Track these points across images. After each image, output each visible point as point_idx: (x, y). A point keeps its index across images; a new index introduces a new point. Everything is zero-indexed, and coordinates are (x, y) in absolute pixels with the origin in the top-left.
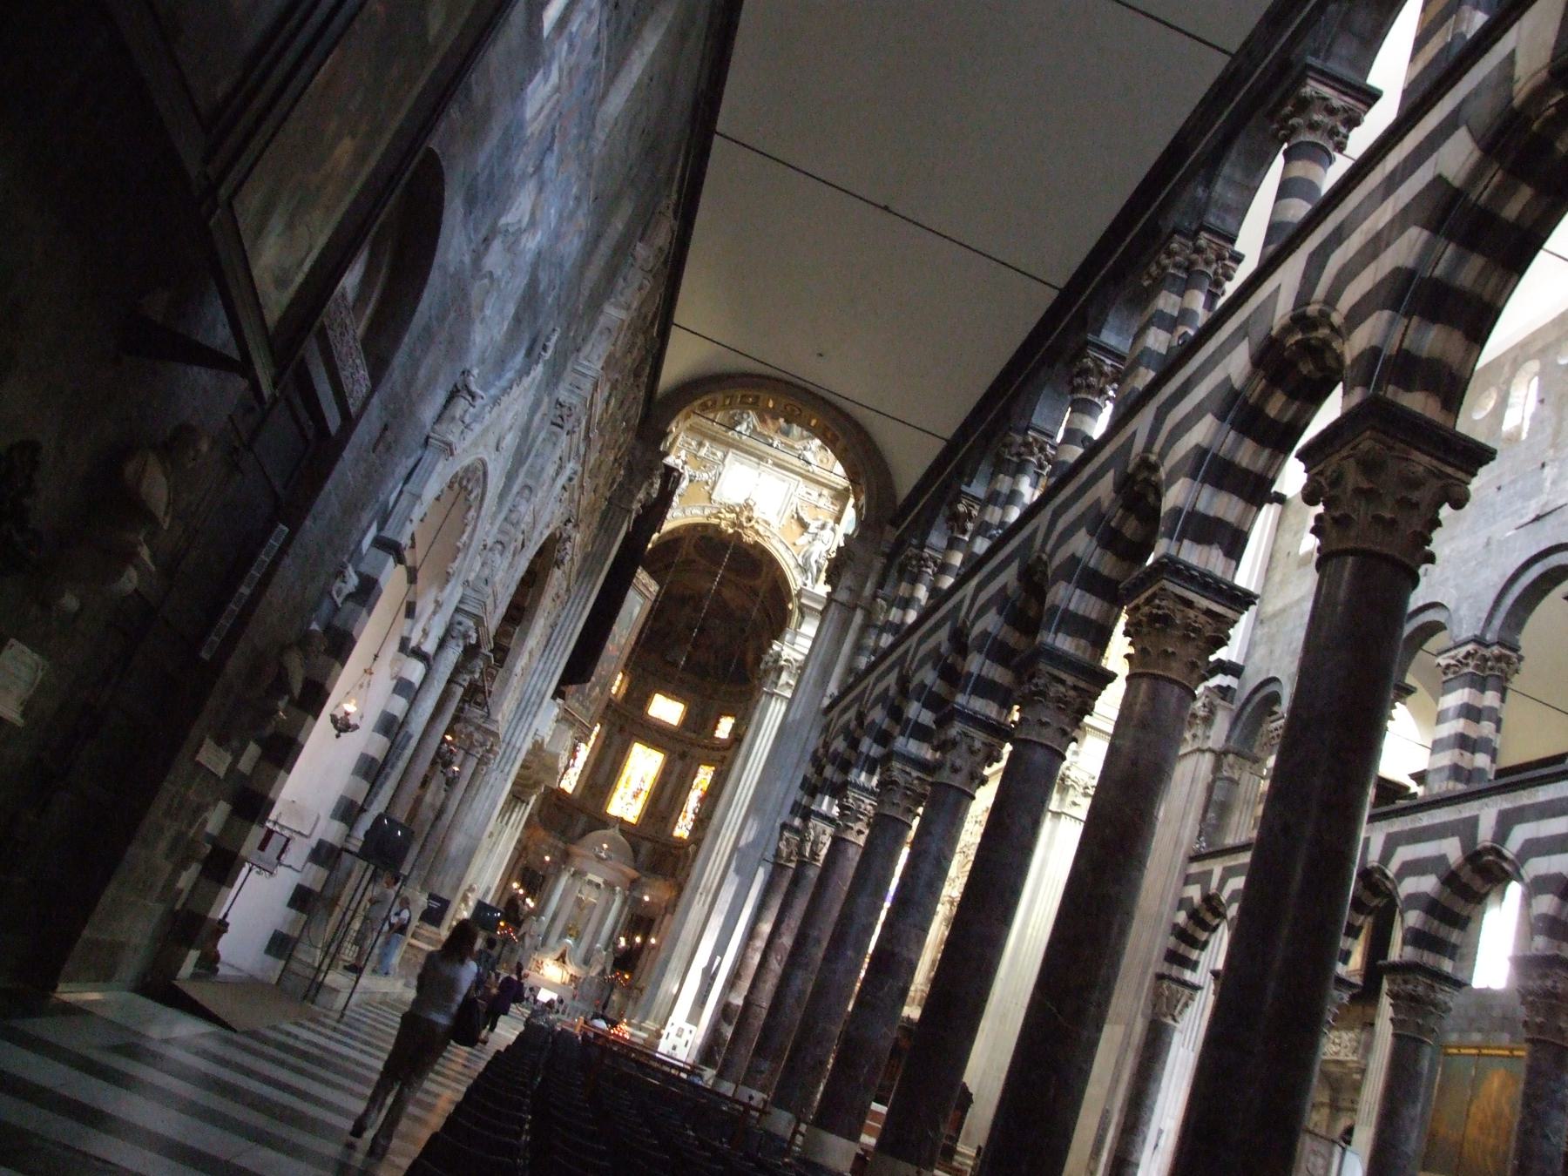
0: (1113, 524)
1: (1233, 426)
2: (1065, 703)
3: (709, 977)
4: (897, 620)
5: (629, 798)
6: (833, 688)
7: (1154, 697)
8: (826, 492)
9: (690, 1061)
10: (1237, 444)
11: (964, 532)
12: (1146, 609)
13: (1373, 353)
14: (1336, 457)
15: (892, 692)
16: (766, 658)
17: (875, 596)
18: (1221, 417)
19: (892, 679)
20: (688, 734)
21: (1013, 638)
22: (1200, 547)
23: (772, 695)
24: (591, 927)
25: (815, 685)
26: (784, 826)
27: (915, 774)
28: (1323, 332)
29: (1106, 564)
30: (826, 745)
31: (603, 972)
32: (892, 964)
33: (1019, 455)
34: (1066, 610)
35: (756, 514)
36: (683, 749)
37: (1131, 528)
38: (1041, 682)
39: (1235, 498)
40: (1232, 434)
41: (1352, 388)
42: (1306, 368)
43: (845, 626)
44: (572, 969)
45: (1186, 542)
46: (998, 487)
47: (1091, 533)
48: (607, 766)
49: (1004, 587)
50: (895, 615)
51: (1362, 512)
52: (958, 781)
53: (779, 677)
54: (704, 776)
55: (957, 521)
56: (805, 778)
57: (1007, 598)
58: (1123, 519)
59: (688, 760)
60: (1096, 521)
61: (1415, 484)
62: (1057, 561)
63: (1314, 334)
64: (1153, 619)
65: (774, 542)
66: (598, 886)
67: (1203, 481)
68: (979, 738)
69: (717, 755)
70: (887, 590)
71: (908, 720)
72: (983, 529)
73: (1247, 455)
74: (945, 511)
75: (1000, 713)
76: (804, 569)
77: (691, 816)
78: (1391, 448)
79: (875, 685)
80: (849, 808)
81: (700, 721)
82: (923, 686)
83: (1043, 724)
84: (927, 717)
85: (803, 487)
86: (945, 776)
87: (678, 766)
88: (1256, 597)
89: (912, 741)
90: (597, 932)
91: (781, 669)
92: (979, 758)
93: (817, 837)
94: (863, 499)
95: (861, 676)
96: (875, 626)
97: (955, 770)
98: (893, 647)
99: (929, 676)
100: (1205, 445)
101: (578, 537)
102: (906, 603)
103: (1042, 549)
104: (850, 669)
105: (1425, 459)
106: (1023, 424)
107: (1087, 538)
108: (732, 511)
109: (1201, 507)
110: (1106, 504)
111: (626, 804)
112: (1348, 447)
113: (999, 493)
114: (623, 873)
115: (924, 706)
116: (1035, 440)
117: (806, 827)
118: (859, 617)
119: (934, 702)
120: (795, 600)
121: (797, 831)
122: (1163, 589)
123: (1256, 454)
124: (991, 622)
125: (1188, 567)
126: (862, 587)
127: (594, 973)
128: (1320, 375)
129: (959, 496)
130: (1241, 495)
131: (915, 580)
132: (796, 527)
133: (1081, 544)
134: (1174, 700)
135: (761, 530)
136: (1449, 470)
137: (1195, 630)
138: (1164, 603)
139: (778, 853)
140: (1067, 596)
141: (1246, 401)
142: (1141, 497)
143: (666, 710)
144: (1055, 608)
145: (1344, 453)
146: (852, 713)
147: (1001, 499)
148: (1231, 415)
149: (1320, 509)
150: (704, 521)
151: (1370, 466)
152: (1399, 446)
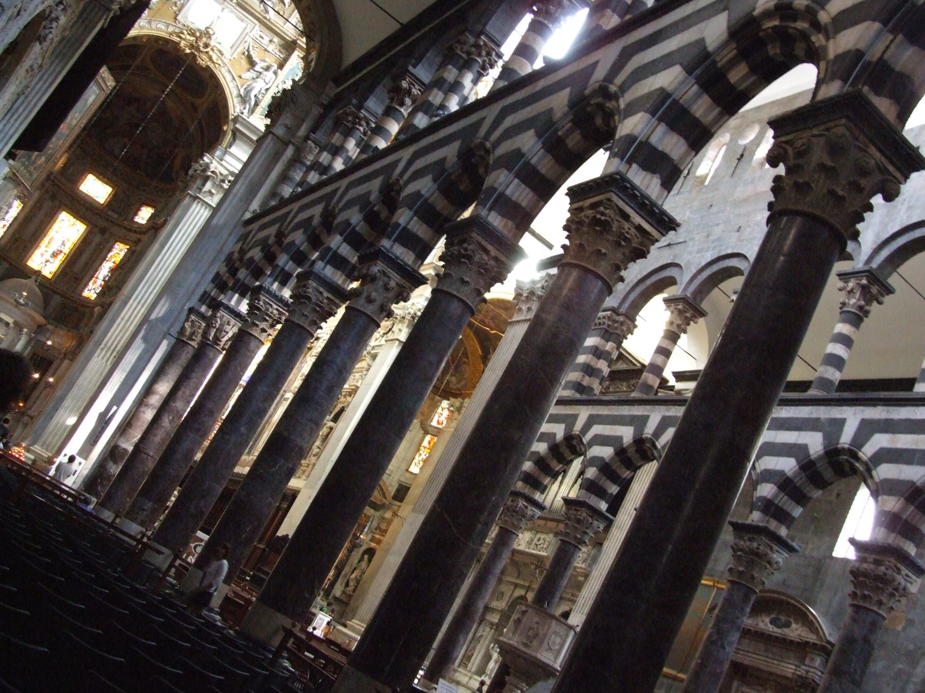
0: (560, 133)
1: (698, 81)
2: (485, 269)
3: (104, 421)
4: (325, 163)
5: (48, 256)
6: (255, 205)
7: (580, 285)
8: (276, 39)
9: (75, 487)
10: (697, 97)
11: (402, 104)
12: (590, 212)
13: (857, 55)
14: (806, 134)
15: (315, 222)
16: (196, 166)
17: (307, 138)
18: (689, 70)
19: (317, 210)
20: (110, 213)
21: (440, 204)
22: (644, 173)
23: (195, 198)
25: (241, 200)
26: (191, 310)
27: (326, 294)
28: (802, 25)
29: (543, 163)
30: (242, 252)
32: (286, 450)
33: (469, 53)
34: (502, 194)
35: (212, 43)
36: (104, 224)
37: (574, 141)
38: (470, 247)
39: (682, 141)
40: (695, 88)
41: (832, 79)
42: (774, 50)
43: (276, 157)
45: (634, 166)
46: (445, 75)
47: (539, 135)
48: (32, 227)
49: (443, 161)
50: (325, 158)
51: (820, 184)
52: (370, 310)
53: (204, 185)
54: (119, 252)
55: (397, 95)
56: (217, 274)
57: (444, 170)
58: (570, 132)
59: (107, 235)
60: (545, 127)
61: (864, 172)
62: (501, 151)
63: (792, 25)
64: (596, 222)
65: (223, 70)
66: (7, 324)
67: (660, 120)
68: (395, 279)
69: (135, 237)
70: (318, 136)
71: (329, 249)
72: (423, 106)
73: (702, 108)
74: (387, 81)
75: (415, 262)
76: (244, 100)
77: (100, 282)
78: (857, 139)
79: (297, 213)
80: (259, 309)
81: (123, 205)
82: (347, 223)
83: (463, 282)
84: (345, 250)
85: (257, 30)
86: (361, 304)
87: (98, 238)
88: (678, 225)
89: (329, 267)
91: (207, 178)
92: (391, 295)
93: (222, 325)
94: (314, 55)
95: (284, 203)
96: (303, 164)
97: (370, 301)
98: (320, 185)
99: (355, 217)
100: (669, 89)
101: (63, 20)
102: (337, 151)
103: (486, 137)
104: (273, 194)
105: (878, 155)
106: (479, 28)
107: (535, 139)
108: (193, 35)
109: (653, 140)
110: (558, 115)
111: (45, 259)
112: (822, 127)
113: (445, 80)
114: (33, 318)
115: (345, 240)
116: (485, 44)
117: (214, 316)
118: (290, 152)
119: (354, 240)
120: (231, 124)
121: (202, 316)
122: (609, 200)
123: (709, 110)
124: (425, 186)
125: (634, 187)
126: (299, 128)
128: (782, 59)
129: (405, 73)
130: (686, 138)
131: (348, 133)
132: (244, 63)
133: (528, 142)
134: (596, 291)
135: (214, 58)
136: (891, 168)
137: (625, 239)
138: (607, 211)
139: (182, 330)
140: (504, 181)
141: (715, 62)
142: (591, 117)
143: (96, 189)
144: (493, 189)
145: (815, 132)
146: (272, 230)
147: (446, 86)
148: (698, 72)
149: (781, 170)
150: (167, 36)
151: (835, 149)
152: (861, 137)
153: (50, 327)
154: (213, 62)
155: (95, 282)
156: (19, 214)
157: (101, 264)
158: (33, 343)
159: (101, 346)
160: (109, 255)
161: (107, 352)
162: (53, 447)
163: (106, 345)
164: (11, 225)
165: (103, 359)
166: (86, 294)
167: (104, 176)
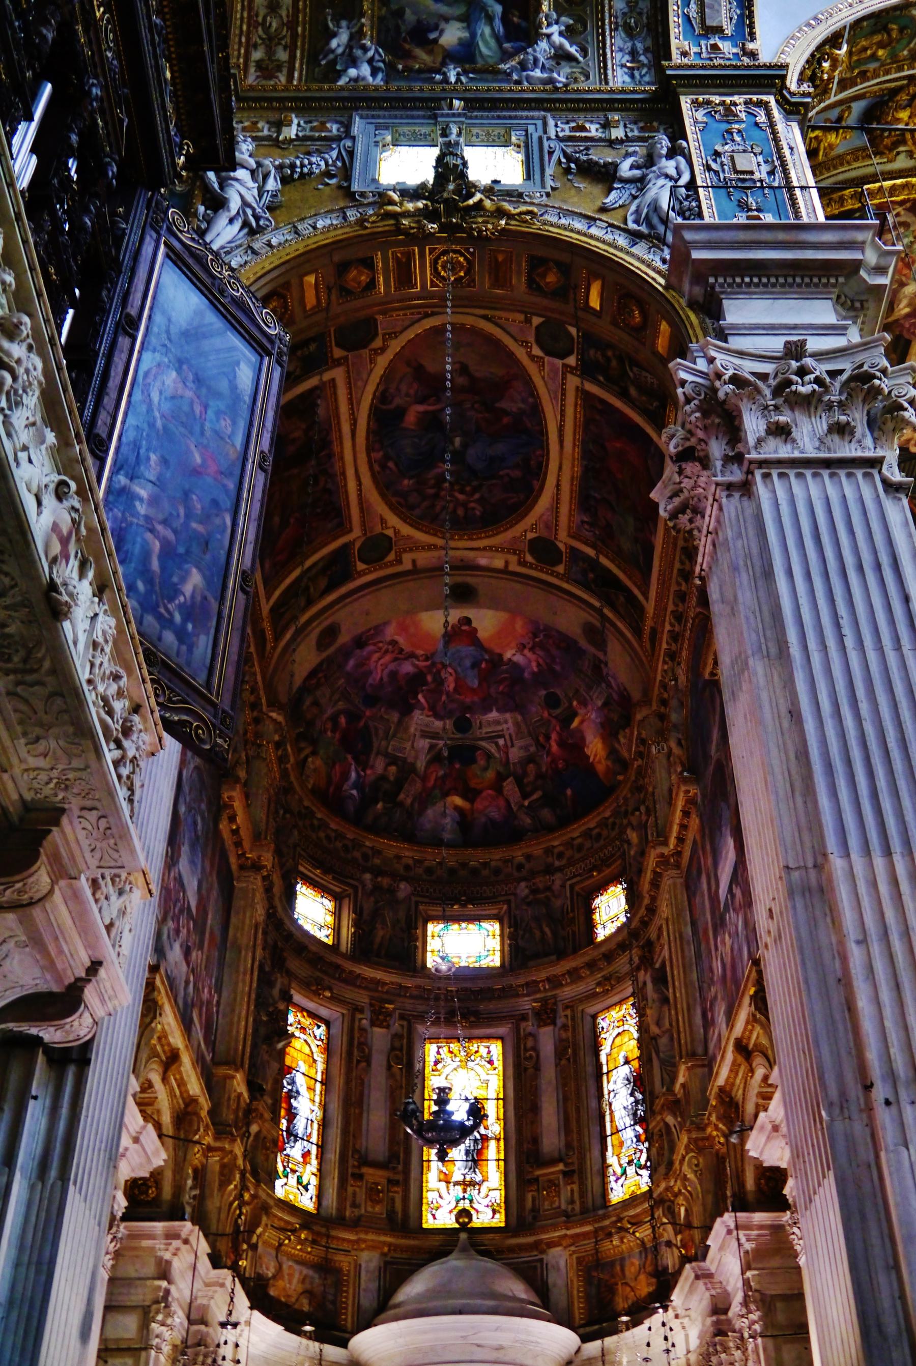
54: (619, 1035)
81: (546, 934)
143: (465, 945)
154: (510, 216)
156: (325, 1107)
157: (602, 1095)
159: (880, 1092)
160: (603, 1059)
164: (321, 1147)
167: (462, 906)
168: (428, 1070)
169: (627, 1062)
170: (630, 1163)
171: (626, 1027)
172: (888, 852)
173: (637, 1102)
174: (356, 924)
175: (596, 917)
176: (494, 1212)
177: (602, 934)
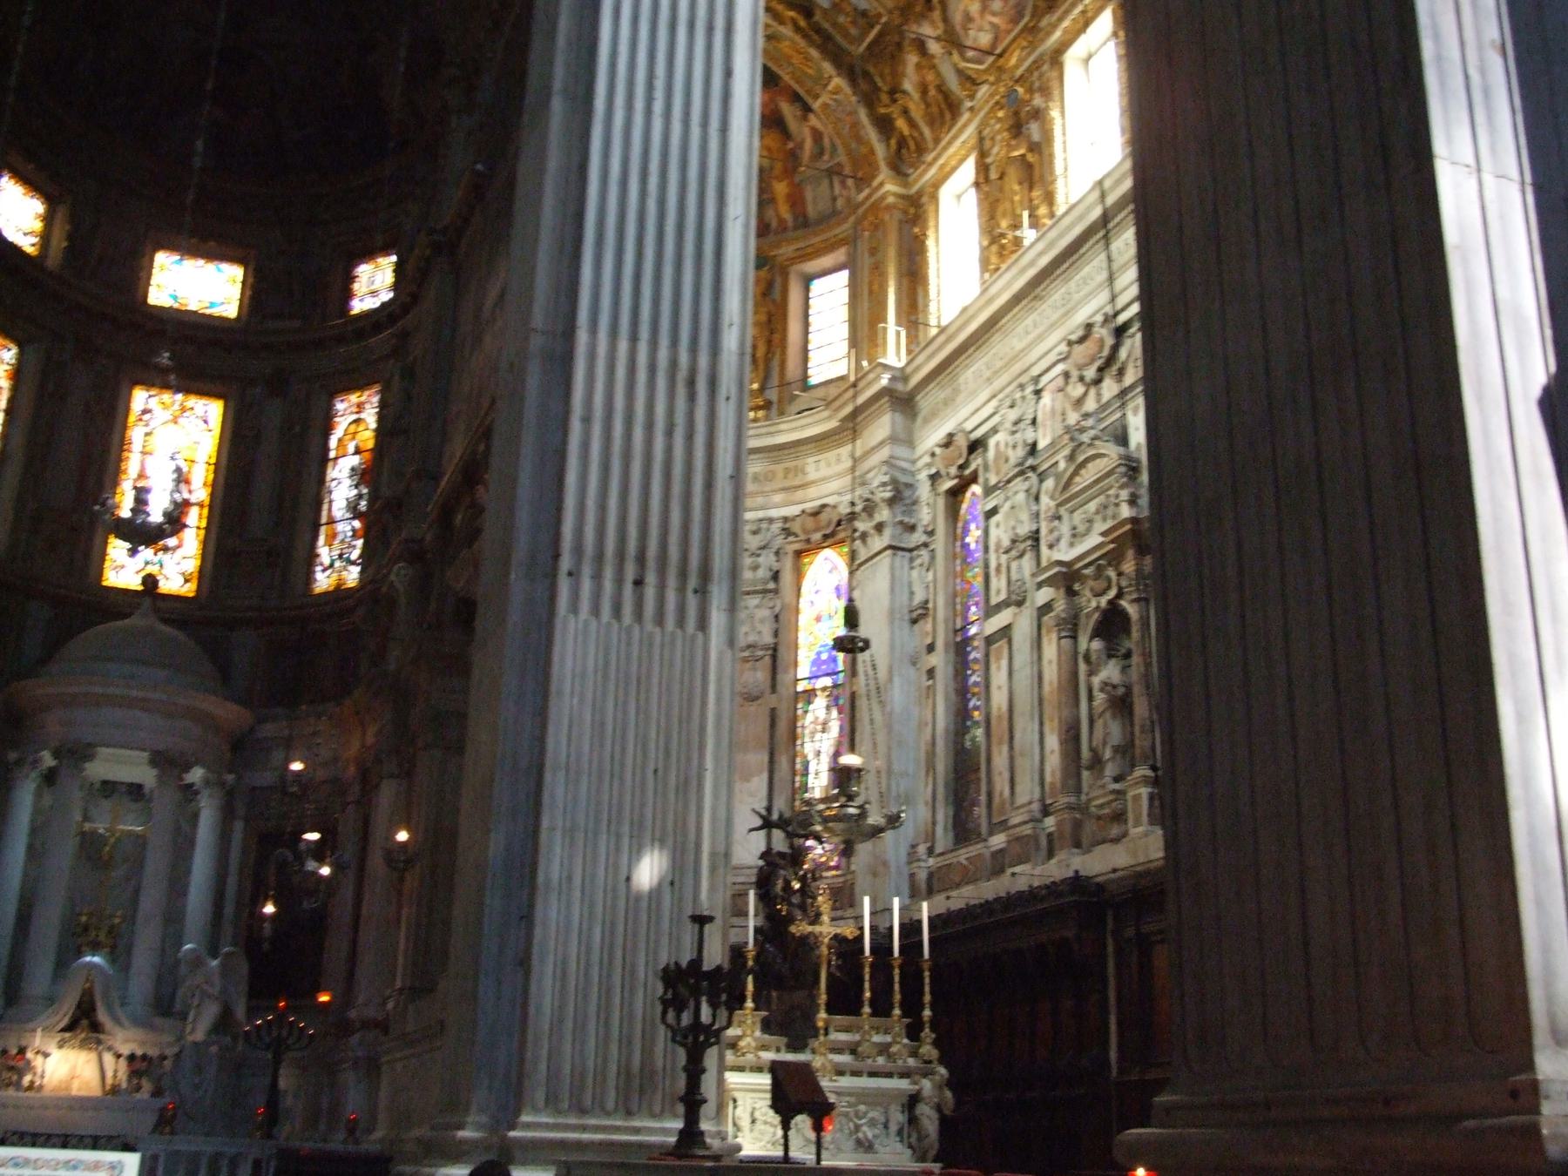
24: (152, 899)
31: (224, 1023)
36: (267, 375)
44: (126, 1041)
54: (355, 421)
66: (135, 791)
81: (294, 292)
90: (173, 919)
127: (199, 1031)
143: (196, 285)
153: (268, 730)
155: (332, 536)
158: (241, 810)
159: (565, 563)
160: (333, 443)
161: (597, 577)
162: (601, 1074)
163: (578, 550)
165: (596, 611)
166: (323, 581)
168: (132, 418)
169: (358, 452)
170: (340, 556)
171: (362, 416)
172: (634, 338)
173: (360, 496)
174: (70, 237)
175: (356, 286)
176: (187, 581)
177: (358, 306)
